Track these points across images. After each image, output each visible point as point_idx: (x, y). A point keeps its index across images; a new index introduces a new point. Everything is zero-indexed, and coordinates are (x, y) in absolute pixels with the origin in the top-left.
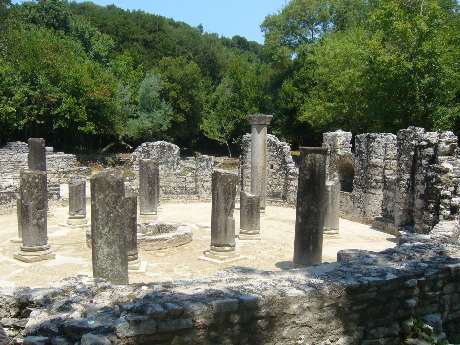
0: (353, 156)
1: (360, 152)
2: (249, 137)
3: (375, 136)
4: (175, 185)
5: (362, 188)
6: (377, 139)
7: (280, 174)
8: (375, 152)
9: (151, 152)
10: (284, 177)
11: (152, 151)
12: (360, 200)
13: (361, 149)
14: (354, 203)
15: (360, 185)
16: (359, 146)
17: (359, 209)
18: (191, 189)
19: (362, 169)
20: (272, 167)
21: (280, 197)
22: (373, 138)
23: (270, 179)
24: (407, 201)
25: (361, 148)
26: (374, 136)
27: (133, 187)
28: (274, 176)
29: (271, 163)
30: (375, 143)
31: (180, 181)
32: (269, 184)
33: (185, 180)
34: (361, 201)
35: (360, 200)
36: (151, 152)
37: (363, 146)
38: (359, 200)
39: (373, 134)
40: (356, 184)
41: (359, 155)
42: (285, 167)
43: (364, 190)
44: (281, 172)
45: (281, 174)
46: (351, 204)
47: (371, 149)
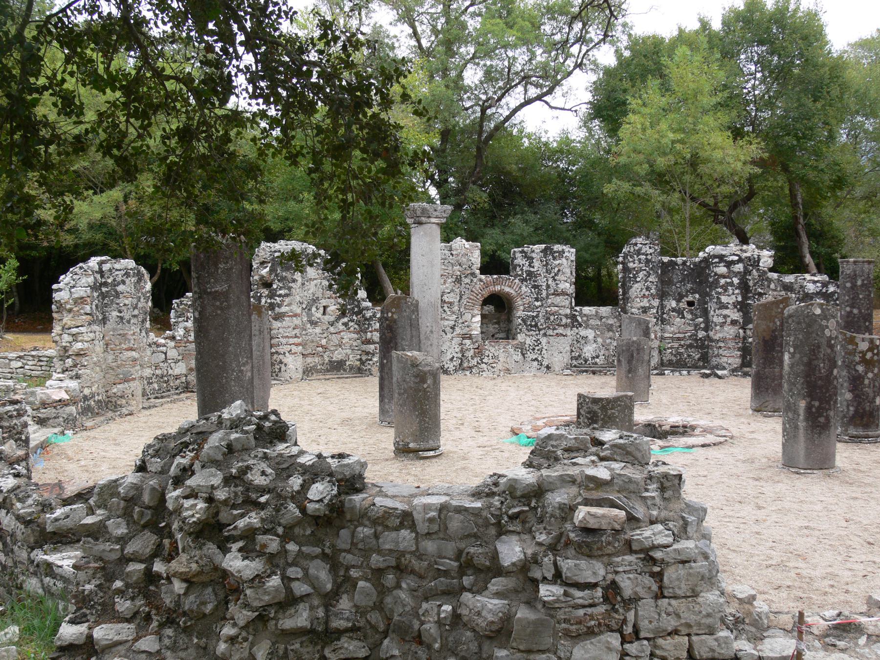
0: (517, 281)
1: (530, 274)
4: (148, 372)
5: (540, 330)
6: (566, 254)
7: (343, 324)
8: (563, 273)
9: (120, 288)
10: (352, 329)
11: (124, 282)
12: (537, 348)
13: (532, 269)
14: (523, 355)
15: (536, 326)
16: (530, 265)
17: (536, 363)
18: (177, 377)
19: (537, 300)
20: (324, 313)
21: (345, 370)
23: (325, 335)
25: (533, 267)
26: (560, 249)
28: (332, 329)
29: (324, 302)
30: (564, 260)
31: (157, 361)
32: (322, 346)
33: (166, 358)
36: (120, 288)
37: (536, 264)
38: (534, 349)
39: (557, 247)
40: (525, 324)
41: (530, 279)
42: (353, 309)
44: (345, 320)
45: (345, 324)
46: (519, 357)
47: (556, 269)
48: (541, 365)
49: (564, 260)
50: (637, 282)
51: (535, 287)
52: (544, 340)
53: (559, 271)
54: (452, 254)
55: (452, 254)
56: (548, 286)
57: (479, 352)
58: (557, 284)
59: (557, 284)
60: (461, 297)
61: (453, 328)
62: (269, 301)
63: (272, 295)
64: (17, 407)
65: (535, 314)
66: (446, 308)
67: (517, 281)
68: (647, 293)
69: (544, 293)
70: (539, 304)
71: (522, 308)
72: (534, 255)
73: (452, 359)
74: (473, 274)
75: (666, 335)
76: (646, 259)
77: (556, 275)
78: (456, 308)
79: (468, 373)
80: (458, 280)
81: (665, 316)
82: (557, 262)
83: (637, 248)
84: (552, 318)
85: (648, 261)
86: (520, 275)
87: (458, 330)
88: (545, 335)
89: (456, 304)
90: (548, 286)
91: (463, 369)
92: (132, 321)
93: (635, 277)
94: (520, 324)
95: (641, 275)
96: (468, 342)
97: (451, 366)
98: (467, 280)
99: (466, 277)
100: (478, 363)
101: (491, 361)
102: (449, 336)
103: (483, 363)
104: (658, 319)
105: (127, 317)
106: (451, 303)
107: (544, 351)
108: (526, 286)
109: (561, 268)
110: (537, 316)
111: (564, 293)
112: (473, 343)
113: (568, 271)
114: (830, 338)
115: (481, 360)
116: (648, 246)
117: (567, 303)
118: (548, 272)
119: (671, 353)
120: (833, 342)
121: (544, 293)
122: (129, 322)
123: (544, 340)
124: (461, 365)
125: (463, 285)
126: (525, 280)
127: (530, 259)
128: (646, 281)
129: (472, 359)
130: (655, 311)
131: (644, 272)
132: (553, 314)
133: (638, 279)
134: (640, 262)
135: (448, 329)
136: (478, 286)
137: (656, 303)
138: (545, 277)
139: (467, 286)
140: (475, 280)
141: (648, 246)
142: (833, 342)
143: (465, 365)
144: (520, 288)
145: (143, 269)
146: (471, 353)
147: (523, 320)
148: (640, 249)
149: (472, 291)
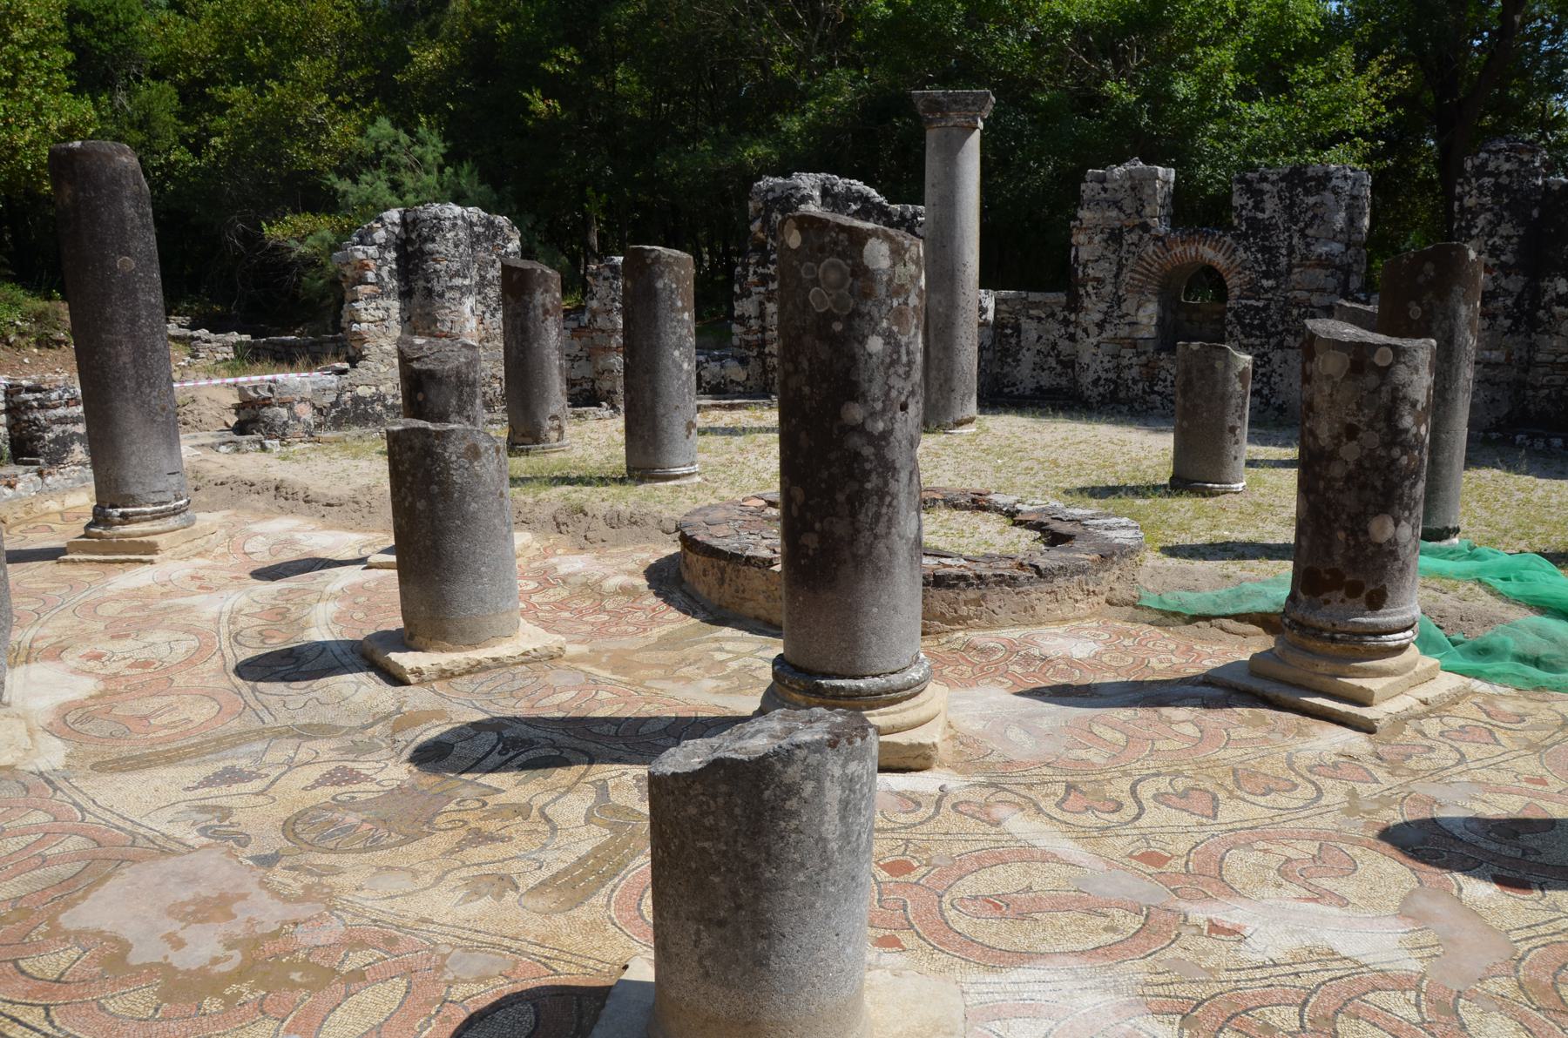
0: (1228, 239)
1: (1253, 223)
2: (797, 188)
3: (1327, 173)
5: (1269, 336)
6: (1334, 182)
9: (429, 246)
11: (433, 240)
12: (1260, 371)
13: (1260, 215)
15: (1262, 327)
19: (1266, 275)
22: (1317, 179)
24: (1515, 356)
25: (1263, 211)
27: (362, 391)
30: (1328, 195)
34: (1263, 375)
35: (1260, 371)
36: (429, 246)
37: (1271, 204)
43: (1273, 341)
47: (1310, 214)
48: (1268, 403)
49: (1328, 195)
50: (1472, 237)
51: (1263, 250)
52: (1276, 357)
53: (1315, 217)
54: (1105, 190)
55: (1105, 190)
56: (1291, 250)
57: (1151, 374)
58: (1308, 245)
59: (1308, 245)
60: (1120, 267)
61: (1101, 326)
62: (761, 270)
63: (763, 263)
64: (38, 395)
65: (1261, 304)
66: (1089, 288)
67: (1228, 239)
68: (1492, 261)
69: (1283, 261)
70: (1267, 283)
71: (1237, 292)
72: (1266, 186)
73: (1096, 382)
74: (1145, 228)
75: (1540, 357)
76: (1496, 184)
77: (1306, 226)
78: (1109, 288)
79: (1125, 409)
80: (1115, 237)
81: (1541, 313)
82: (1311, 200)
83: (1477, 162)
84: (1295, 312)
85: (1498, 189)
86: (1235, 228)
87: (1109, 332)
88: (1280, 345)
89: (1110, 279)
90: (1291, 250)
91: (1119, 402)
92: (447, 295)
93: (1469, 227)
94: (1230, 322)
95: (1481, 221)
96: (1128, 353)
97: (1093, 393)
98: (1134, 237)
99: (1130, 232)
100: (1144, 391)
101: (1169, 390)
102: (1094, 340)
103: (1154, 392)
104: (1517, 322)
105: (438, 288)
106: (1098, 280)
107: (1275, 378)
108: (1246, 249)
109: (1319, 211)
110: (1266, 308)
111: (1324, 262)
112: (1138, 355)
113: (1340, 219)
114: (829, 317)
115: (1151, 387)
116: (1502, 157)
117: (1332, 283)
118: (1294, 219)
119: (1548, 397)
120: (838, 327)
121: (1283, 261)
122: (441, 296)
123: (1276, 357)
124: (1114, 393)
125: (1125, 247)
126: (1245, 236)
127: (1257, 195)
128: (1491, 236)
129: (1135, 382)
130: (1509, 302)
131: (1489, 215)
132: (1298, 305)
133: (1475, 232)
134: (1481, 193)
135: (1094, 330)
136: (1151, 248)
137: (1515, 283)
138: (1288, 229)
139: (1133, 248)
140: (1146, 236)
141: (1502, 157)
142: (838, 327)
143: (1122, 395)
144: (1235, 250)
145: (502, 220)
146: (1135, 372)
147: (1236, 315)
148: (1485, 163)
149: (1141, 258)
